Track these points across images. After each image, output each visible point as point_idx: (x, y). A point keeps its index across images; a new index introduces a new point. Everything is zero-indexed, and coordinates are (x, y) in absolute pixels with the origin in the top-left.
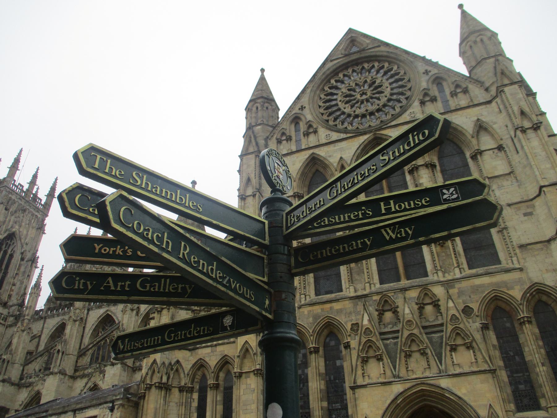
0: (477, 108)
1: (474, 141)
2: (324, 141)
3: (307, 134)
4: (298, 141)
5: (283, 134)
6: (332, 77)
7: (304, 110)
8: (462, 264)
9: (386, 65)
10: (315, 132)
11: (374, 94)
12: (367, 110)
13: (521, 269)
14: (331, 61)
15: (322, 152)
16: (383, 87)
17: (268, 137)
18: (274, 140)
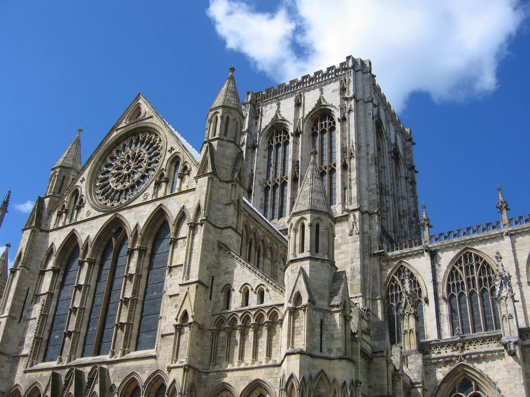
0: (189, 194)
1: (172, 229)
2: (85, 218)
3: (79, 209)
4: (73, 213)
5: (64, 206)
6: (115, 147)
7: (84, 182)
8: (129, 346)
9: (154, 137)
10: (83, 206)
11: (136, 168)
12: (124, 186)
13: (154, 357)
14: (117, 130)
15: (78, 229)
16: (143, 162)
17: (51, 210)
18: (56, 213)
